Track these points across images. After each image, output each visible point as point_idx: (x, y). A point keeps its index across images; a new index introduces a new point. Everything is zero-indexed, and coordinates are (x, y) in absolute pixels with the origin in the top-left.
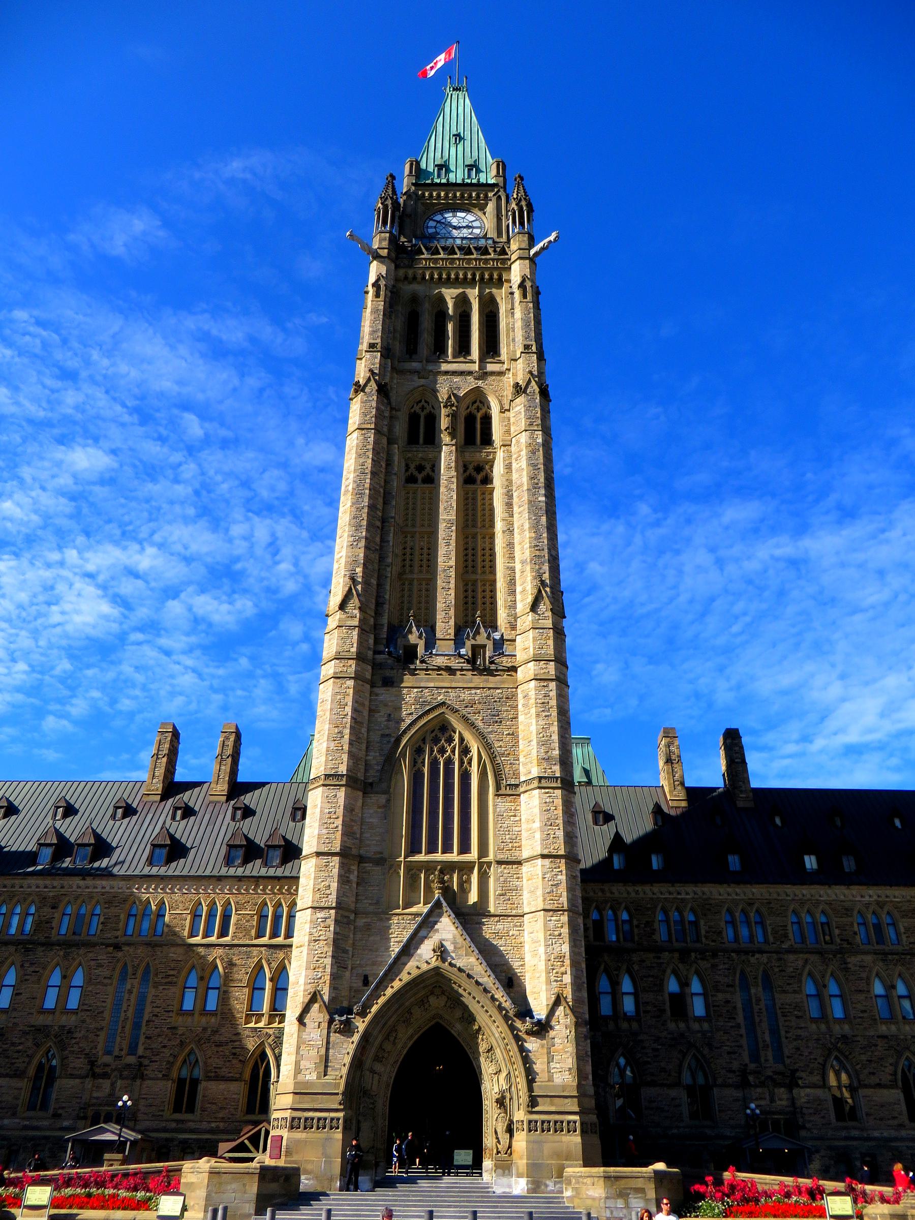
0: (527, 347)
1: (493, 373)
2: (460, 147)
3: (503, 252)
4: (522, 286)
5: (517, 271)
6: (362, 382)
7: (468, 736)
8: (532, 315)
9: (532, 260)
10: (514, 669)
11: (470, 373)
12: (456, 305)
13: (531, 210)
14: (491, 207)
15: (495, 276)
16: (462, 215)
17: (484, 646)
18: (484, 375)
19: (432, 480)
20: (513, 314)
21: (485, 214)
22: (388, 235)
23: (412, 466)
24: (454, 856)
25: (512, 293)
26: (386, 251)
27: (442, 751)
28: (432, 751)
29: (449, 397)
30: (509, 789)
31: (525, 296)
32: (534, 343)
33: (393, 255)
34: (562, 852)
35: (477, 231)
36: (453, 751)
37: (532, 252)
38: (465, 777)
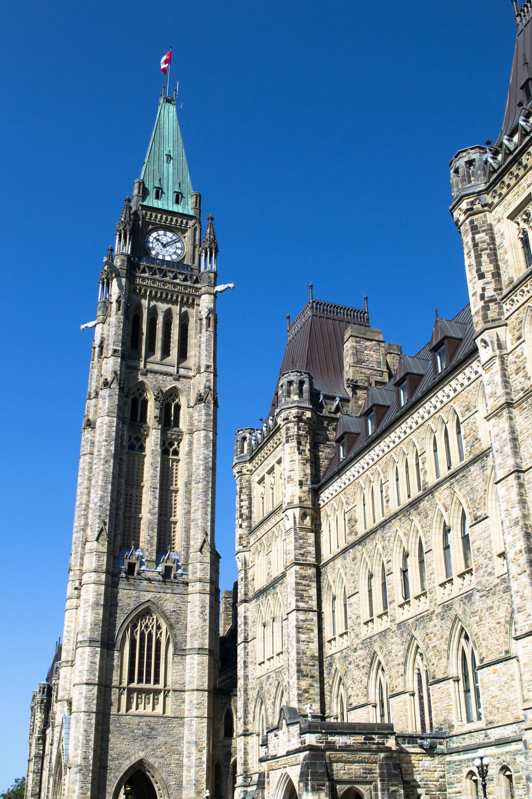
0: (208, 367)
1: (185, 377)
3: (197, 281)
4: (208, 318)
5: (205, 302)
6: (109, 379)
7: (162, 621)
9: (215, 295)
10: (187, 584)
11: (171, 375)
13: (217, 251)
14: (189, 234)
17: (172, 567)
18: (178, 378)
19: (142, 448)
23: (133, 438)
24: (151, 686)
25: (201, 320)
27: (147, 627)
28: (141, 627)
29: (158, 393)
30: (180, 652)
32: (212, 364)
34: (206, 688)
35: (179, 251)
36: (152, 627)
38: (158, 642)
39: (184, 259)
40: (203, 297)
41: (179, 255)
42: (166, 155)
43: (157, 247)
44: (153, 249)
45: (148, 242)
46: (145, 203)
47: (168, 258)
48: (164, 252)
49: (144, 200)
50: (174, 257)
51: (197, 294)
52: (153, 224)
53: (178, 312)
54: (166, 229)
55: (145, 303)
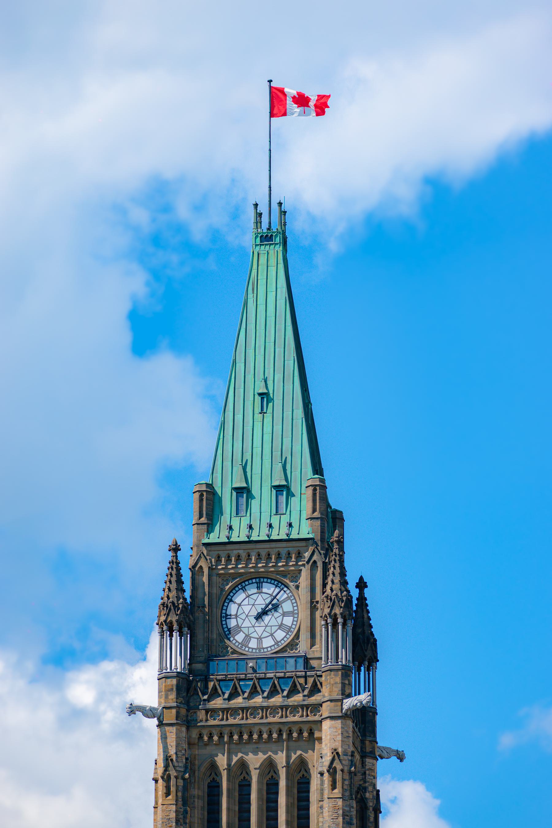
2: (268, 418)
3: (315, 689)
4: (332, 771)
8: (341, 819)
12: (260, 776)
15: (305, 734)
16: (269, 589)
20: (321, 807)
21: (297, 587)
22: (174, 681)
25: (322, 774)
26: (174, 711)
31: (334, 787)
33: (183, 711)
35: (288, 621)
37: (348, 703)
39: (297, 636)
40: (326, 725)
41: (288, 630)
42: (260, 394)
43: (247, 624)
44: (238, 628)
45: (228, 616)
46: (213, 538)
47: (268, 643)
48: (260, 630)
49: (210, 527)
50: (280, 635)
51: (317, 718)
52: (234, 576)
53: (284, 764)
54: (259, 579)
55: (222, 761)
